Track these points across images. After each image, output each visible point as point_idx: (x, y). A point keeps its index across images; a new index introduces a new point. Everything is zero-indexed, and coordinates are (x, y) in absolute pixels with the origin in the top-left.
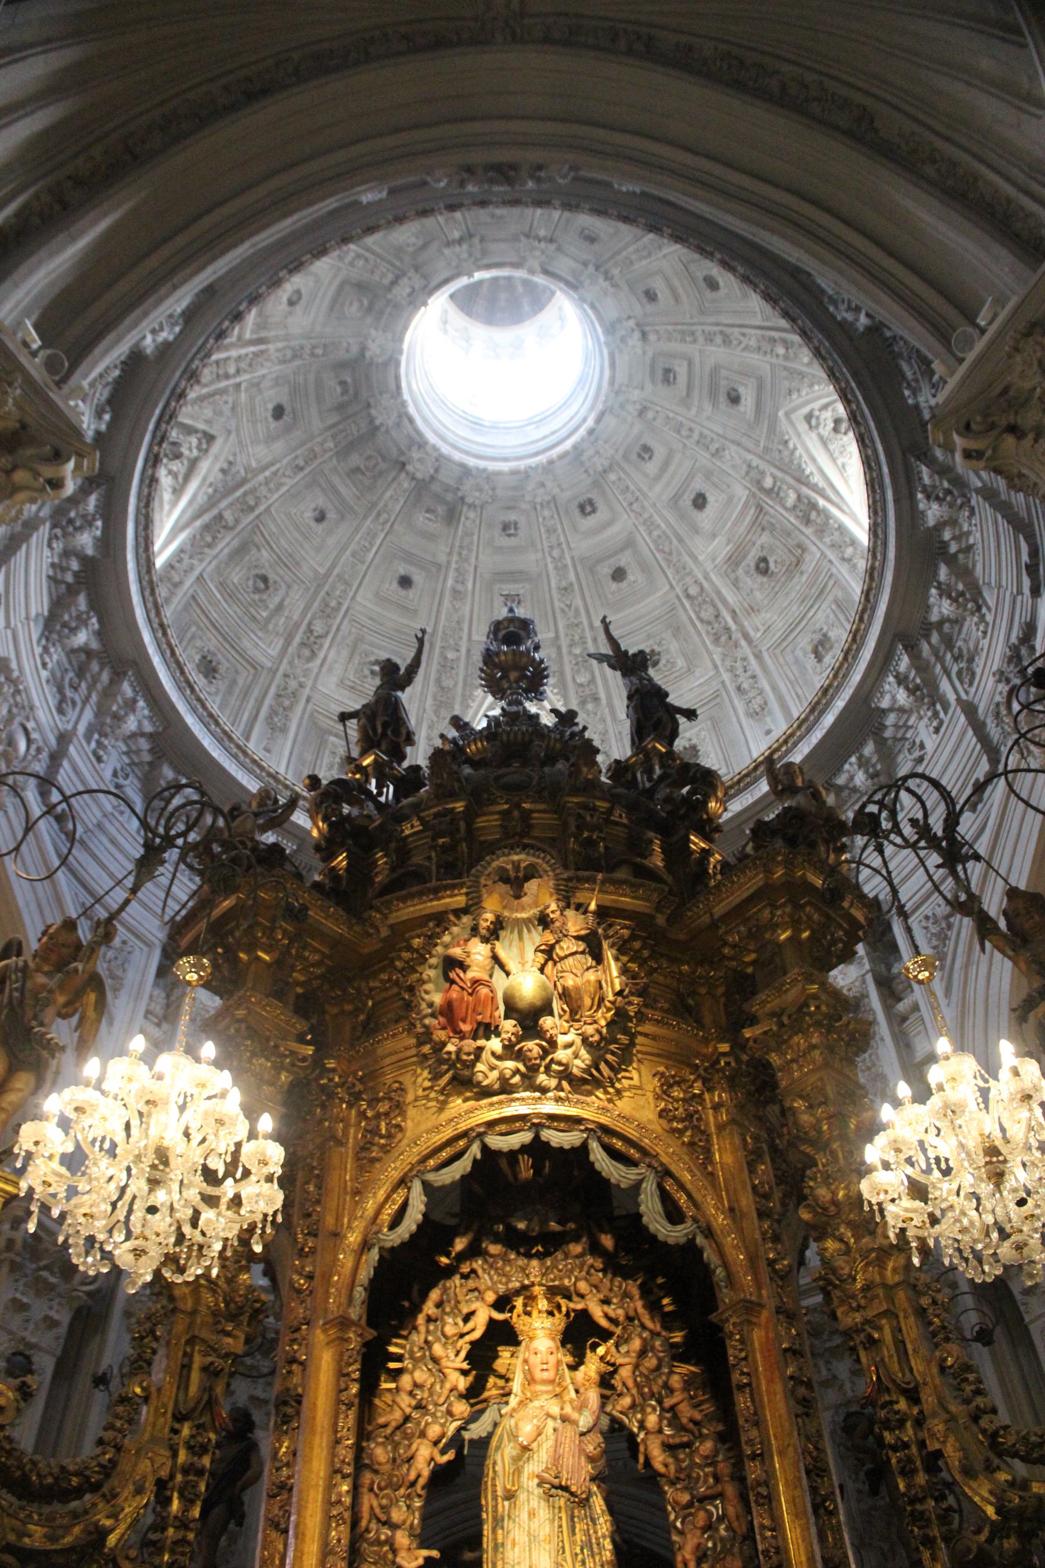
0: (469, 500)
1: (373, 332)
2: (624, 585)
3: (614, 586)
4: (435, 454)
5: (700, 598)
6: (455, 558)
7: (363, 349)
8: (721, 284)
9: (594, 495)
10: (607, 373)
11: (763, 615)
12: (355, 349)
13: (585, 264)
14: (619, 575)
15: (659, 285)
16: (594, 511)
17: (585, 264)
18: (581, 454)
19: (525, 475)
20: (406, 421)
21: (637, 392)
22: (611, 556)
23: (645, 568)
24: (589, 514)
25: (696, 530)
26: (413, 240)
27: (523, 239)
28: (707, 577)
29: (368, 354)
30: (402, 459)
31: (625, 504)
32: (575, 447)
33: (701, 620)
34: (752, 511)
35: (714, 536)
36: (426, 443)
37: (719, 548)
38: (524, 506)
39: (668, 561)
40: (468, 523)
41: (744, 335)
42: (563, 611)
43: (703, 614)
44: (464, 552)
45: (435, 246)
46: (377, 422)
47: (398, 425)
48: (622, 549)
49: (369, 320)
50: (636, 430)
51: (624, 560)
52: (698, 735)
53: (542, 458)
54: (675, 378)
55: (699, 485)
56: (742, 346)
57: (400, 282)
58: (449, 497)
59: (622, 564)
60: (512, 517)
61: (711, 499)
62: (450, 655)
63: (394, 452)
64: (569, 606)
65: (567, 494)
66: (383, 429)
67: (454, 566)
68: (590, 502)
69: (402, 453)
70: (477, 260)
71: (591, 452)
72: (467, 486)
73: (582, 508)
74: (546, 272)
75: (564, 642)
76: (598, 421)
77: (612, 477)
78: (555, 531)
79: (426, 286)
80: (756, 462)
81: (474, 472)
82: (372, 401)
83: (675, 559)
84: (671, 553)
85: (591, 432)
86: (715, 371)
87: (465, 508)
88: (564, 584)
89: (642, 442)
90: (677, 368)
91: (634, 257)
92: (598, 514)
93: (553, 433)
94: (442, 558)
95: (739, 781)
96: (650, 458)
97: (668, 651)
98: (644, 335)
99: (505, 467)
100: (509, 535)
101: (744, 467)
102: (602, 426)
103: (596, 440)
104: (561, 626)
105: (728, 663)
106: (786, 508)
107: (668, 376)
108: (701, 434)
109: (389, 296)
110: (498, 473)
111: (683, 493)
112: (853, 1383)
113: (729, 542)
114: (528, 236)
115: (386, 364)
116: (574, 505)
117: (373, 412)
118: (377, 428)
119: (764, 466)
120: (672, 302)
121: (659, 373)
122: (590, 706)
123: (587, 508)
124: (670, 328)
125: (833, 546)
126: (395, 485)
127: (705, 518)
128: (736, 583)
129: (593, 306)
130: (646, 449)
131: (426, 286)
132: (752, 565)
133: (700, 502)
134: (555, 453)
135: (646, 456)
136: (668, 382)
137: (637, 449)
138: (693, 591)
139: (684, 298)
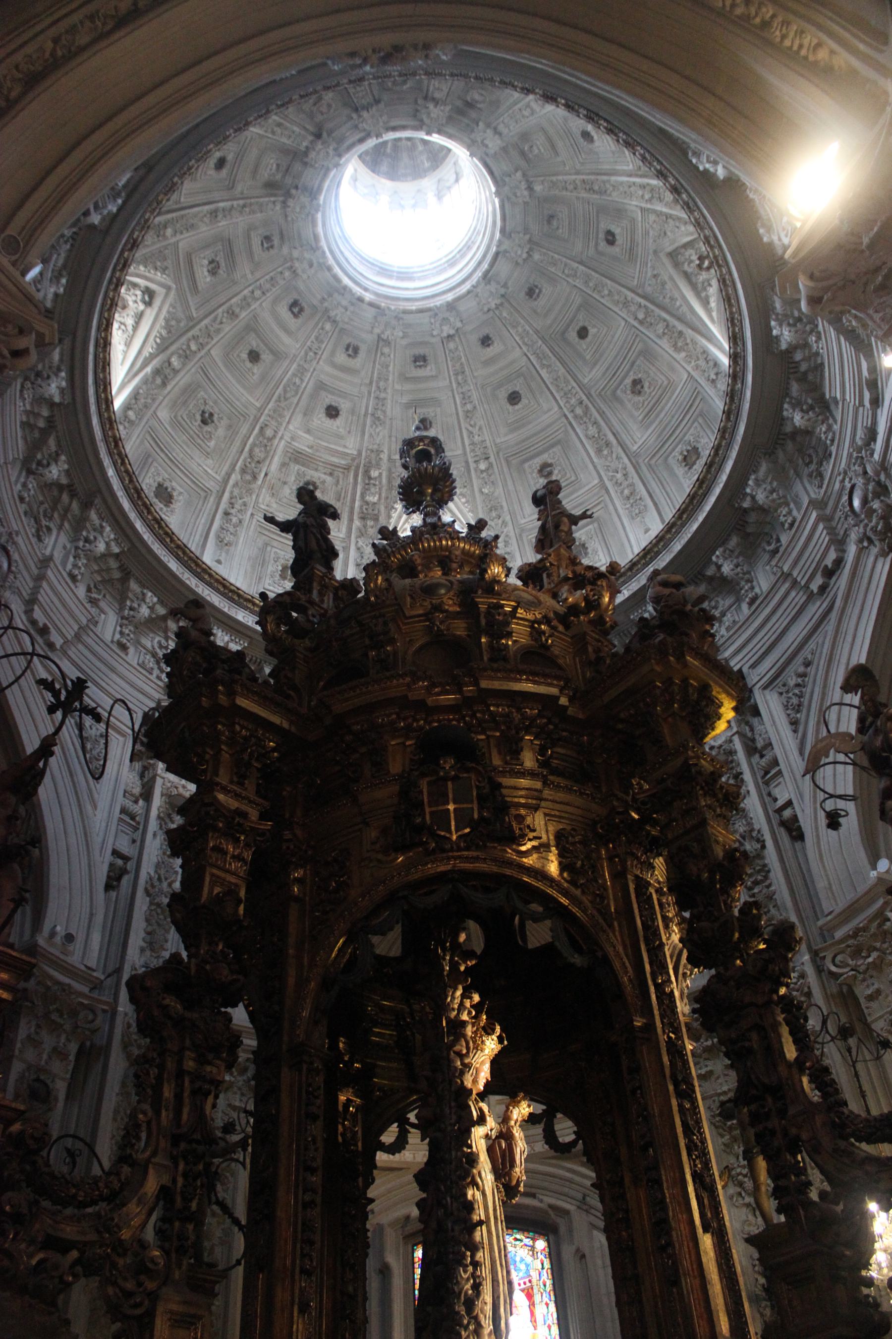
0: (290, 202)
1: (448, 108)
2: (248, 364)
3: (244, 356)
4: (331, 166)
5: (266, 442)
6: (241, 202)
7: (436, 102)
8: (517, 407)
9: (307, 311)
10: (413, 306)
11: (273, 500)
12: (437, 95)
13: (505, 286)
14: (254, 356)
15: (496, 348)
16: (296, 316)
17: (505, 286)
18: (339, 293)
19: (315, 248)
20: (362, 134)
21: (401, 334)
22: (266, 345)
23: (263, 377)
24: (293, 312)
25: (308, 413)
26: (536, 151)
27: (527, 237)
28: (281, 438)
29: (431, 106)
30: (325, 135)
31: (309, 343)
32: (345, 288)
33: (251, 451)
34: (343, 462)
35: (308, 431)
36: (340, 156)
37: (305, 441)
38: (285, 250)
39: (279, 397)
40: (271, 206)
41: (480, 429)
42: (216, 318)
43: (257, 450)
44: (247, 210)
45: (523, 163)
46: (365, 114)
47: (356, 127)
48: (272, 352)
49: (459, 103)
50: (364, 336)
51: (266, 357)
52: (180, 493)
53: (331, 261)
54: (420, 366)
55: (344, 406)
56: (470, 429)
57: (497, 136)
58: (289, 180)
59: (263, 356)
60: (276, 242)
61: (339, 421)
62: (169, 232)
63: (330, 125)
64: (221, 323)
65: (301, 286)
66: (354, 116)
67: (235, 203)
68: (301, 310)
69: (330, 133)
70: (508, 199)
71: (344, 303)
72: (304, 199)
73: (295, 303)
74: (497, 254)
75: (195, 331)
76: (371, 304)
77: (328, 326)
78: (273, 285)
79: (487, 155)
80: (384, 456)
81: (315, 202)
82: (382, 105)
83: (283, 404)
84: (286, 399)
85: (361, 300)
86: (436, 402)
87: (281, 199)
88: (237, 310)
89: (360, 344)
90: (429, 368)
91: (520, 329)
92: (293, 320)
93: (347, 260)
94: (239, 188)
95: (231, 591)
96: (349, 356)
97: (216, 428)
98: (449, 337)
99: (320, 229)
100: (262, 244)
101: (375, 447)
102: (365, 306)
103: (353, 304)
104: (206, 322)
105: (236, 492)
106: (363, 496)
107: (420, 360)
108: (385, 399)
109: (481, 124)
110: (314, 223)
111: (333, 394)
112: (50, 1058)
113: (311, 447)
114: (530, 241)
115: (415, 114)
116: (296, 297)
117: (374, 108)
118: (356, 110)
119: (385, 464)
120: (483, 359)
121: (420, 351)
122: (159, 381)
123: (296, 308)
124: (463, 359)
125: (358, 549)
126: (303, 132)
127: (320, 420)
128: (284, 465)
129: (469, 292)
130: (356, 350)
131: (487, 155)
132: (308, 478)
133: (332, 412)
134: (337, 270)
135: (350, 352)
136: (415, 361)
137: (355, 342)
138: (269, 433)
139: (492, 369)
